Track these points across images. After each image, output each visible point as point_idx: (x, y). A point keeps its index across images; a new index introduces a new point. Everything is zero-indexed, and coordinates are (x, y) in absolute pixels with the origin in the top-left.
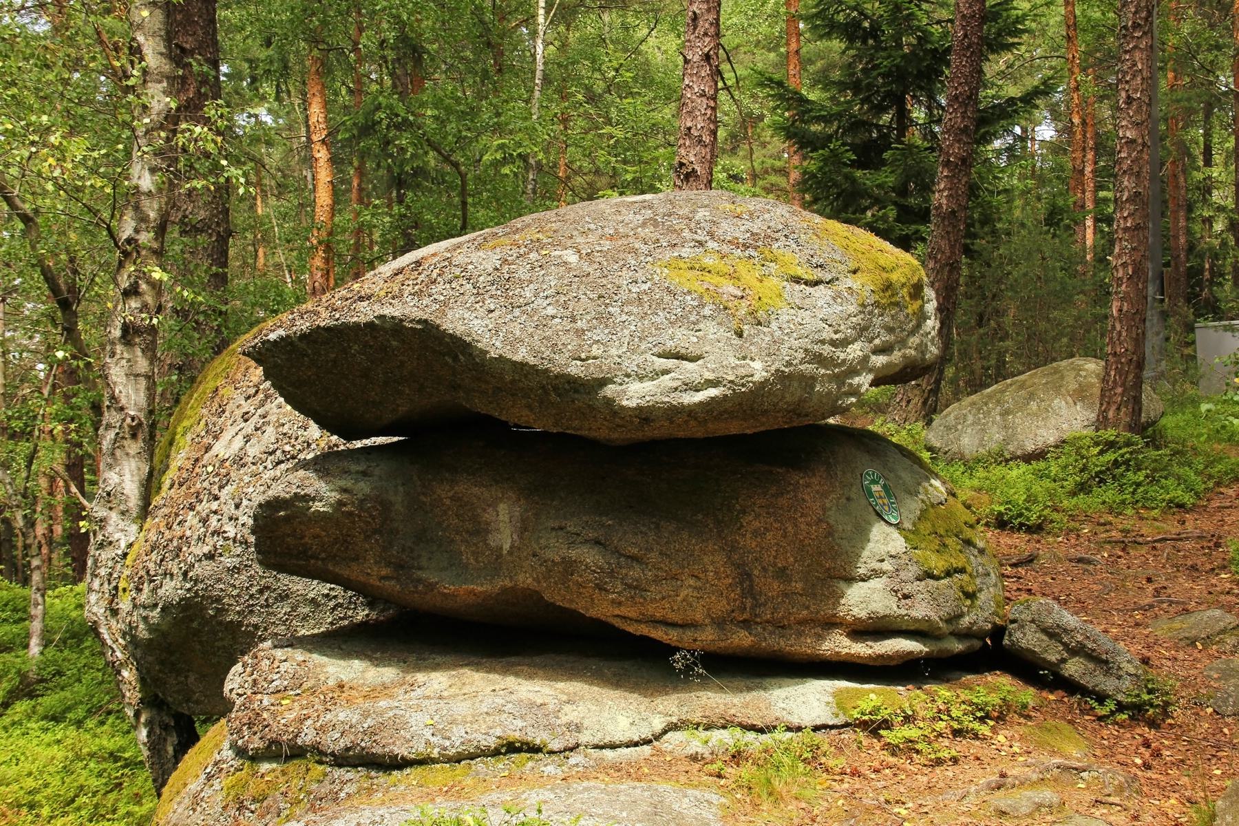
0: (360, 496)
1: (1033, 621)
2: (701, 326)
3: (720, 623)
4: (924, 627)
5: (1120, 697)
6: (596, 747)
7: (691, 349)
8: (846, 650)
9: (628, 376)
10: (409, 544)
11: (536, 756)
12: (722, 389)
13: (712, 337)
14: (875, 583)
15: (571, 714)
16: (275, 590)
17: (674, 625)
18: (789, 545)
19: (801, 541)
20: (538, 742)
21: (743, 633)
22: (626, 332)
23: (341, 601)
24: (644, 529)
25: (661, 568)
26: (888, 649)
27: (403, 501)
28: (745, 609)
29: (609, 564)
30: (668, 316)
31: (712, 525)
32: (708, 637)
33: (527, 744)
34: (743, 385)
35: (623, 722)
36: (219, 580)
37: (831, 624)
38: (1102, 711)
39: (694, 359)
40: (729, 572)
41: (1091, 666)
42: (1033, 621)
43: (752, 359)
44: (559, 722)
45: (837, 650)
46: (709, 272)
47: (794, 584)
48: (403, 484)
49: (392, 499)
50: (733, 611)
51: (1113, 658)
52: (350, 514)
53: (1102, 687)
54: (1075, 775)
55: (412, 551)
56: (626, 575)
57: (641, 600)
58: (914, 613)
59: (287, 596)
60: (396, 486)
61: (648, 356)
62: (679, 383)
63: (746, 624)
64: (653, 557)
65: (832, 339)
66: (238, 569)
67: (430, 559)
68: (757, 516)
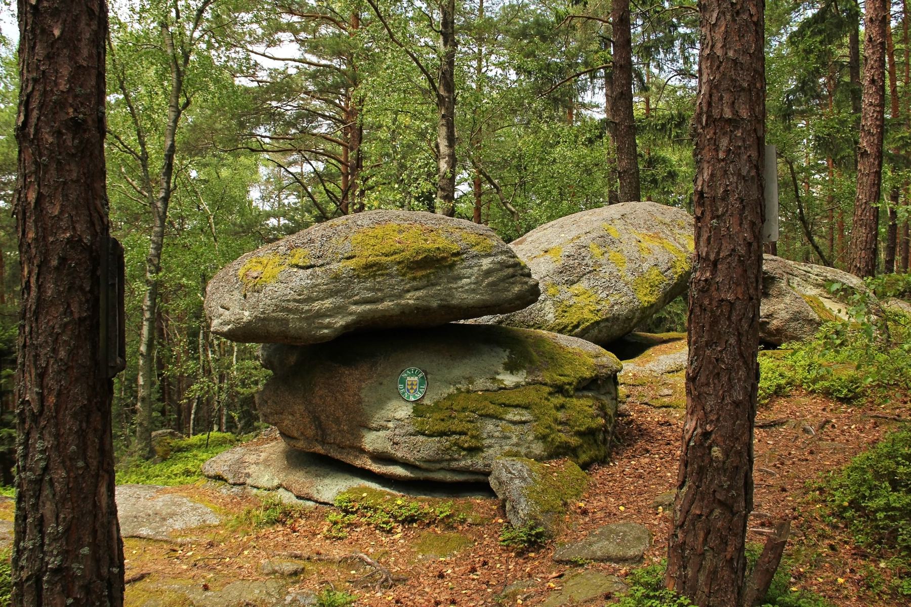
2: (233, 293)
6: (252, 486)
14: (382, 433)
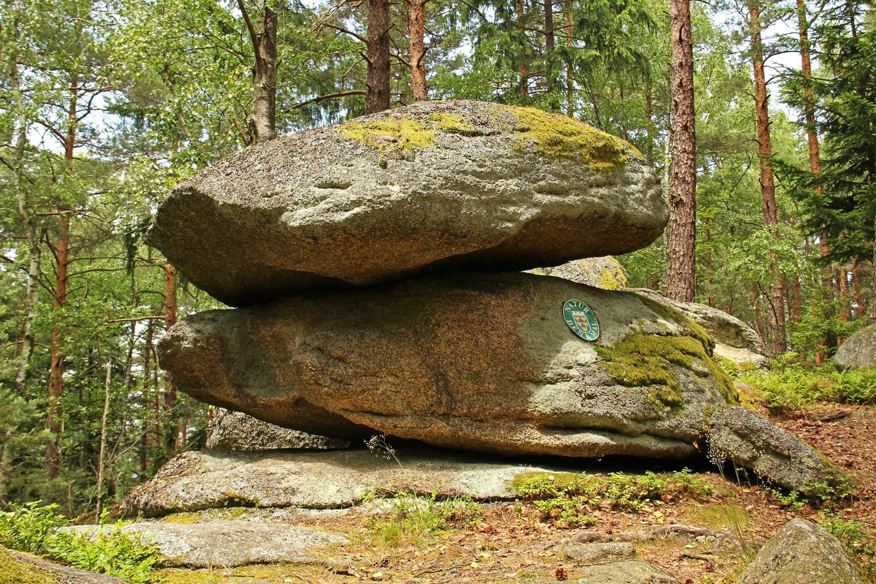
0: (207, 335)
1: (726, 425)
2: (353, 162)
3: (421, 415)
4: (609, 424)
5: (802, 489)
6: (305, 507)
7: (341, 179)
8: (537, 441)
9: (296, 204)
10: (243, 370)
11: (250, 510)
12: (363, 207)
13: (360, 169)
15: (293, 481)
16: (266, 434)
17: (379, 415)
18: (482, 352)
19: (493, 350)
20: (252, 498)
21: (441, 424)
22: (300, 173)
23: (307, 442)
24: (350, 337)
25: (360, 366)
26: (575, 441)
27: (236, 338)
28: (441, 403)
29: (320, 363)
30: (330, 158)
31: (411, 336)
32: (406, 426)
33: (244, 499)
34: (381, 203)
35: (333, 489)
36: (235, 427)
37: (523, 419)
38: (785, 501)
39: (344, 187)
40: (424, 373)
41: (777, 461)
42: (726, 425)
43: (392, 184)
44: (278, 486)
45: (527, 440)
46: (380, 129)
47: (487, 385)
48: (238, 327)
49: (228, 336)
50: (432, 406)
51: (794, 453)
52: (202, 348)
53: (786, 480)
54: (692, 538)
55: (244, 374)
56: (333, 372)
57: (345, 392)
58: (597, 411)
59: (274, 438)
60: (232, 328)
61: (312, 188)
62: (331, 205)
63: (446, 416)
64: (353, 357)
65: (475, 171)
66: (245, 419)
67: (255, 380)
68: (450, 329)
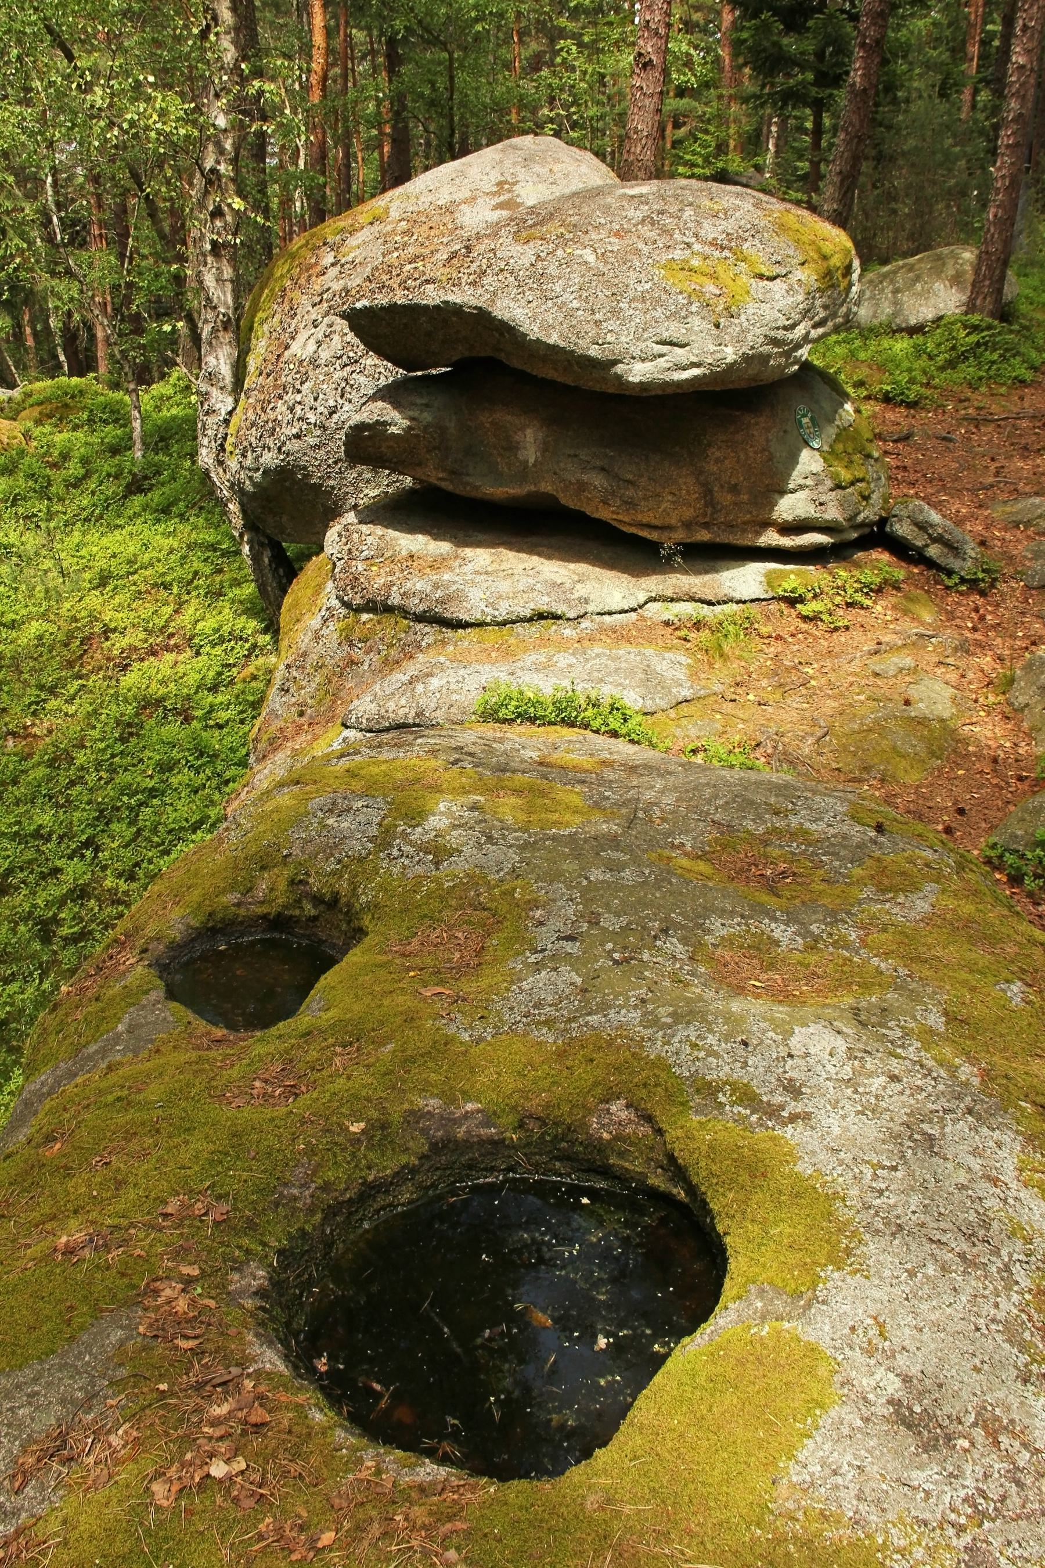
2: (689, 320)
3: (688, 525)
4: (832, 525)
6: (599, 614)
9: (634, 358)
14: (801, 495)
15: (581, 591)
17: (655, 528)
21: (704, 532)
36: (305, 454)
37: (767, 524)
41: (946, 550)
52: (417, 436)
61: (649, 343)
63: (706, 526)
68: (719, 448)
